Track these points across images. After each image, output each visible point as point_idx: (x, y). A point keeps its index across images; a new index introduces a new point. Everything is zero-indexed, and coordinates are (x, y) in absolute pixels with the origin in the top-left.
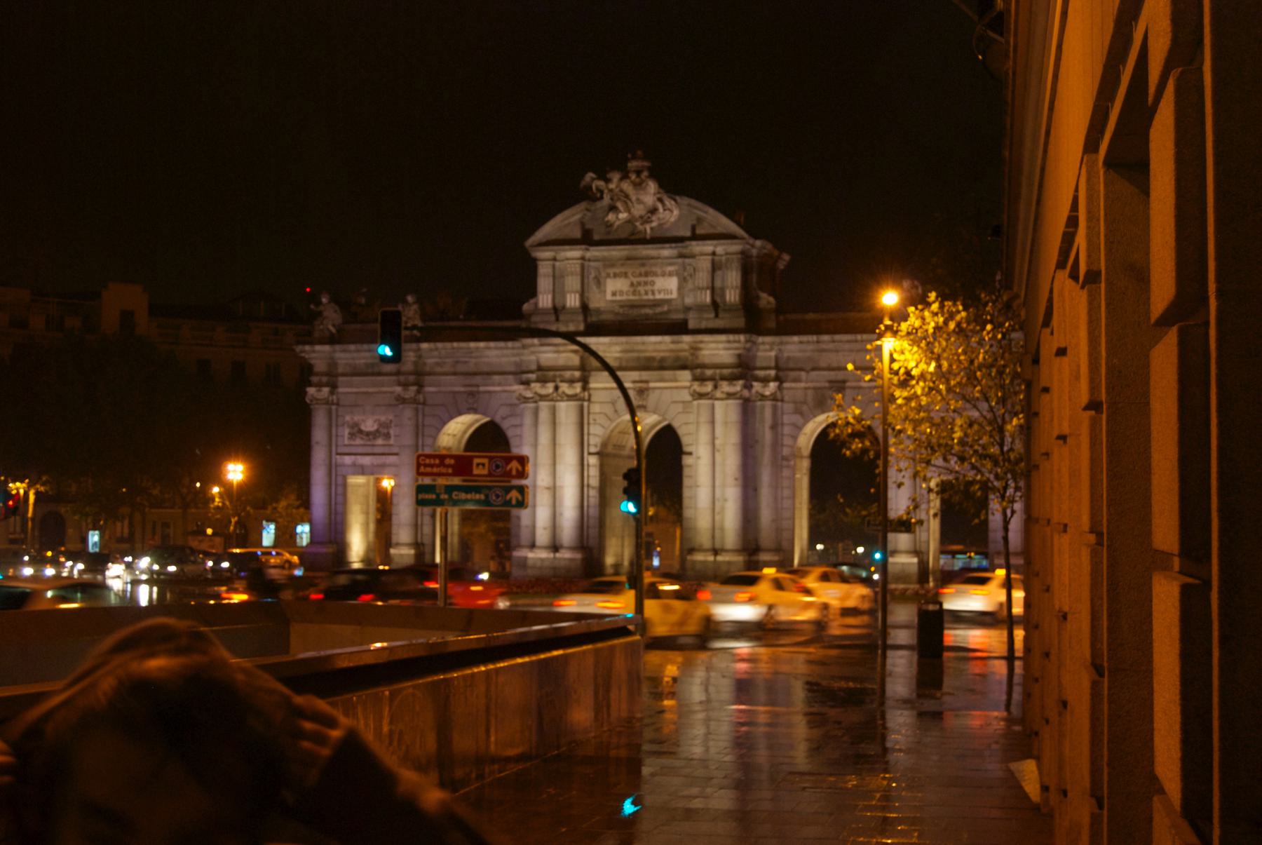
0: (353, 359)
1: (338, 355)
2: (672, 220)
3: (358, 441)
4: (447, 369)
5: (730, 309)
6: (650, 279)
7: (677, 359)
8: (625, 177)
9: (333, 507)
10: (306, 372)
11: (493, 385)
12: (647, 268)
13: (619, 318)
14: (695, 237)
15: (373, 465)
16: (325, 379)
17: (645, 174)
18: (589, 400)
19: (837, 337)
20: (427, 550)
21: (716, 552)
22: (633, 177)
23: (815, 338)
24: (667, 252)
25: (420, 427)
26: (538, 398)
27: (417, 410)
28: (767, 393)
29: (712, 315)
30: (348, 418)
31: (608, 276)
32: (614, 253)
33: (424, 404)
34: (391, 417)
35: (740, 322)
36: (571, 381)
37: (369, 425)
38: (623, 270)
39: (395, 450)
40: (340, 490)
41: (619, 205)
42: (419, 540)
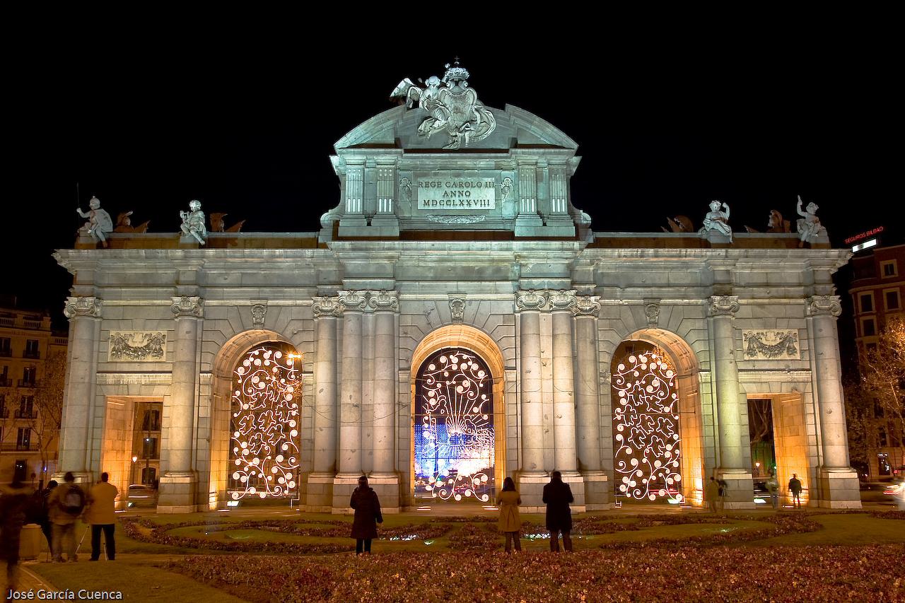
2: (490, 132)
3: (124, 358)
5: (558, 217)
7: (498, 270)
8: (443, 85)
10: (64, 282)
11: (284, 299)
14: (516, 146)
17: (466, 84)
22: (451, 85)
24: (484, 162)
25: (199, 343)
30: (113, 333)
31: (420, 184)
33: (203, 317)
34: (163, 333)
35: (572, 232)
37: (138, 341)
38: (436, 179)
39: (169, 368)
41: (437, 114)
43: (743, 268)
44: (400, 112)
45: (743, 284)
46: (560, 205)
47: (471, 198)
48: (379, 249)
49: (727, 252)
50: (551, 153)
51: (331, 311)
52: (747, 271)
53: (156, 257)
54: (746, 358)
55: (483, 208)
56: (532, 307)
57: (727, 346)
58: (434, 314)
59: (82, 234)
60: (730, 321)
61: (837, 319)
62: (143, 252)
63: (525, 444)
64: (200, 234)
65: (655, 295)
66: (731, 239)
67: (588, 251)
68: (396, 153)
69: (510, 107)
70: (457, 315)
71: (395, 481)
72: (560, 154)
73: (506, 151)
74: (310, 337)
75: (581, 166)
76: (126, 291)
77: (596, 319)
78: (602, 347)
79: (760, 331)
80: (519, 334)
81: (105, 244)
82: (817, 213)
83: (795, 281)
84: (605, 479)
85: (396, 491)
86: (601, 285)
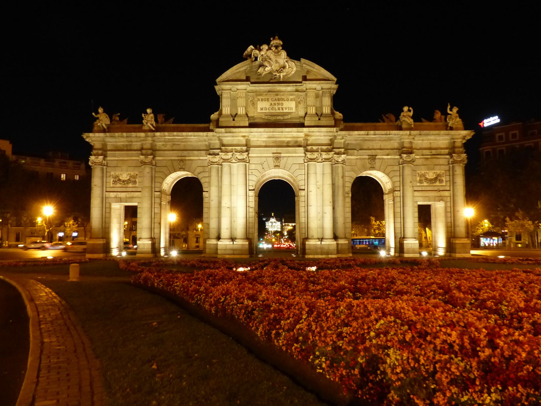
0: (116, 142)
1: (108, 139)
2: (293, 73)
3: (118, 185)
4: (168, 147)
5: (326, 116)
6: (281, 102)
7: (296, 142)
8: (270, 49)
9: (104, 219)
10: (88, 149)
11: (194, 156)
12: (279, 97)
13: (266, 121)
15: (127, 198)
16: (100, 152)
17: (281, 48)
18: (249, 163)
19: (377, 132)
20: (157, 241)
21: (322, 239)
22: (273, 49)
23: (366, 132)
24: (290, 88)
25: (153, 178)
26: (222, 161)
27: (152, 168)
28: (340, 160)
29: (318, 119)
30: (112, 173)
31: (259, 100)
32: (262, 88)
33: (155, 165)
34: (137, 173)
35: (333, 123)
36: (242, 152)
40: (108, 210)
41: (266, 64)
42: (153, 236)
43: (419, 140)
44: (248, 63)
45: (418, 148)
46: (327, 110)
47: (284, 106)
48: (239, 132)
49: (410, 132)
50: (323, 83)
51: (217, 162)
52: (420, 142)
53: (131, 137)
54: (418, 184)
55: (289, 111)
56: (312, 160)
57: (408, 179)
58: (265, 164)
59: (95, 125)
60: (411, 166)
61: (464, 165)
62: (125, 134)
63: (309, 225)
64: (152, 125)
65: (374, 154)
66: (413, 126)
67: (340, 133)
68: (247, 84)
69: (303, 60)
70: (277, 164)
71: (247, 243)
72: (327, 83)
73: (301, 82)
74: (206, 175)
75: (338, 90)
76: (118, 153)
77: (344, 166)
78: (347, 179)
79: (426, 172)
80: (306, 173)
81: (107, 130)
82: (458, 112)
83: (445, 146)
84: (347, 242)
85: (247, 247)
86: (347, 149)
